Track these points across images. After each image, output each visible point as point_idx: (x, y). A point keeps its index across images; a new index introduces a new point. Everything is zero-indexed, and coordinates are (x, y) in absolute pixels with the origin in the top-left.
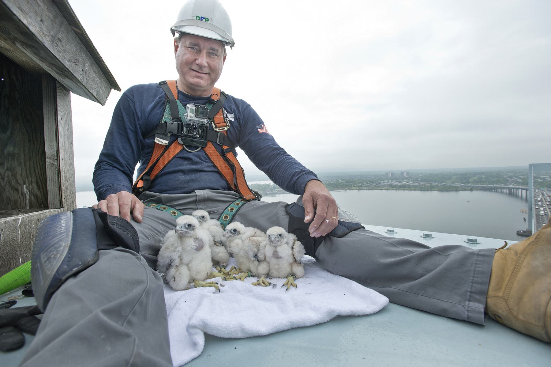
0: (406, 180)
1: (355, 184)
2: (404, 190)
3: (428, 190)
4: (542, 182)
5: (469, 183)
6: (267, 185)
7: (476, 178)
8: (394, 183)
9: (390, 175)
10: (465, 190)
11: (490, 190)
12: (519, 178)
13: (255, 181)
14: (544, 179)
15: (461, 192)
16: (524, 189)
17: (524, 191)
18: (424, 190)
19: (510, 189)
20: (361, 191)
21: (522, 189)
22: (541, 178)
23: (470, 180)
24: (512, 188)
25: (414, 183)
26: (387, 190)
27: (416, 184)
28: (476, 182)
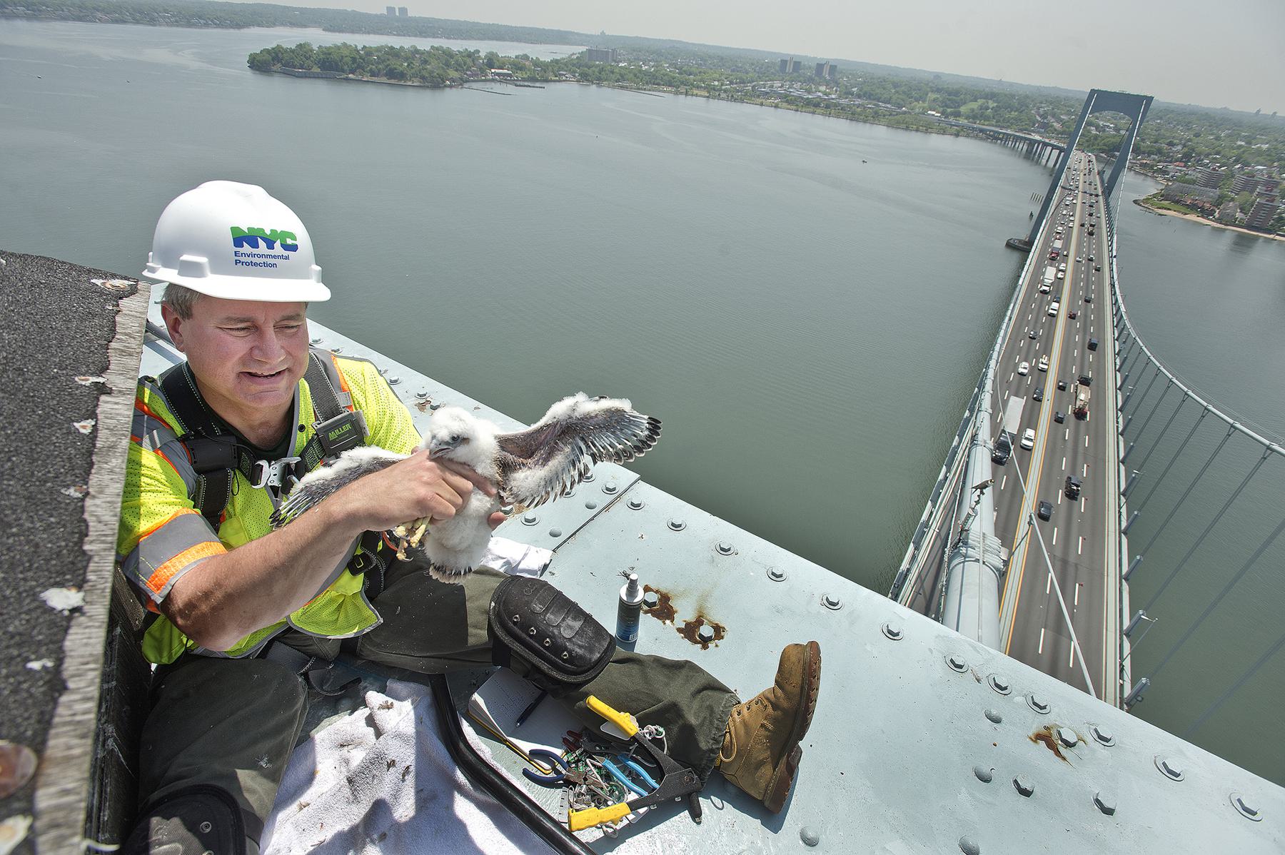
0: (823, 88)
1: (702, 80)
2: (814, 113)
3: (865, 122)
4: (1096, 137)
5: (957, 115)
6: (470, 55)
7: (974, 105)
8: (797, 91)
9: (789, 68)
10: (944, 133)
11: (994, 138)
12: (1059, 120)
13: (434, 36)
14: (1103, 129)
15: (934, 135)
16: (1058, 148)
17: (1056, 152)
18: (857, 120)
19: (1032, 143)
20: (714, 103)
21: (1054, 147)
22: (1097, 127)
23: (963, 109)
24: (1036, 141)
25: (840, 97)
26: (776, 107)
27: (843, 101)
28: (973, 116)
